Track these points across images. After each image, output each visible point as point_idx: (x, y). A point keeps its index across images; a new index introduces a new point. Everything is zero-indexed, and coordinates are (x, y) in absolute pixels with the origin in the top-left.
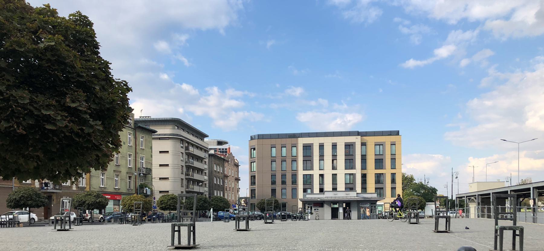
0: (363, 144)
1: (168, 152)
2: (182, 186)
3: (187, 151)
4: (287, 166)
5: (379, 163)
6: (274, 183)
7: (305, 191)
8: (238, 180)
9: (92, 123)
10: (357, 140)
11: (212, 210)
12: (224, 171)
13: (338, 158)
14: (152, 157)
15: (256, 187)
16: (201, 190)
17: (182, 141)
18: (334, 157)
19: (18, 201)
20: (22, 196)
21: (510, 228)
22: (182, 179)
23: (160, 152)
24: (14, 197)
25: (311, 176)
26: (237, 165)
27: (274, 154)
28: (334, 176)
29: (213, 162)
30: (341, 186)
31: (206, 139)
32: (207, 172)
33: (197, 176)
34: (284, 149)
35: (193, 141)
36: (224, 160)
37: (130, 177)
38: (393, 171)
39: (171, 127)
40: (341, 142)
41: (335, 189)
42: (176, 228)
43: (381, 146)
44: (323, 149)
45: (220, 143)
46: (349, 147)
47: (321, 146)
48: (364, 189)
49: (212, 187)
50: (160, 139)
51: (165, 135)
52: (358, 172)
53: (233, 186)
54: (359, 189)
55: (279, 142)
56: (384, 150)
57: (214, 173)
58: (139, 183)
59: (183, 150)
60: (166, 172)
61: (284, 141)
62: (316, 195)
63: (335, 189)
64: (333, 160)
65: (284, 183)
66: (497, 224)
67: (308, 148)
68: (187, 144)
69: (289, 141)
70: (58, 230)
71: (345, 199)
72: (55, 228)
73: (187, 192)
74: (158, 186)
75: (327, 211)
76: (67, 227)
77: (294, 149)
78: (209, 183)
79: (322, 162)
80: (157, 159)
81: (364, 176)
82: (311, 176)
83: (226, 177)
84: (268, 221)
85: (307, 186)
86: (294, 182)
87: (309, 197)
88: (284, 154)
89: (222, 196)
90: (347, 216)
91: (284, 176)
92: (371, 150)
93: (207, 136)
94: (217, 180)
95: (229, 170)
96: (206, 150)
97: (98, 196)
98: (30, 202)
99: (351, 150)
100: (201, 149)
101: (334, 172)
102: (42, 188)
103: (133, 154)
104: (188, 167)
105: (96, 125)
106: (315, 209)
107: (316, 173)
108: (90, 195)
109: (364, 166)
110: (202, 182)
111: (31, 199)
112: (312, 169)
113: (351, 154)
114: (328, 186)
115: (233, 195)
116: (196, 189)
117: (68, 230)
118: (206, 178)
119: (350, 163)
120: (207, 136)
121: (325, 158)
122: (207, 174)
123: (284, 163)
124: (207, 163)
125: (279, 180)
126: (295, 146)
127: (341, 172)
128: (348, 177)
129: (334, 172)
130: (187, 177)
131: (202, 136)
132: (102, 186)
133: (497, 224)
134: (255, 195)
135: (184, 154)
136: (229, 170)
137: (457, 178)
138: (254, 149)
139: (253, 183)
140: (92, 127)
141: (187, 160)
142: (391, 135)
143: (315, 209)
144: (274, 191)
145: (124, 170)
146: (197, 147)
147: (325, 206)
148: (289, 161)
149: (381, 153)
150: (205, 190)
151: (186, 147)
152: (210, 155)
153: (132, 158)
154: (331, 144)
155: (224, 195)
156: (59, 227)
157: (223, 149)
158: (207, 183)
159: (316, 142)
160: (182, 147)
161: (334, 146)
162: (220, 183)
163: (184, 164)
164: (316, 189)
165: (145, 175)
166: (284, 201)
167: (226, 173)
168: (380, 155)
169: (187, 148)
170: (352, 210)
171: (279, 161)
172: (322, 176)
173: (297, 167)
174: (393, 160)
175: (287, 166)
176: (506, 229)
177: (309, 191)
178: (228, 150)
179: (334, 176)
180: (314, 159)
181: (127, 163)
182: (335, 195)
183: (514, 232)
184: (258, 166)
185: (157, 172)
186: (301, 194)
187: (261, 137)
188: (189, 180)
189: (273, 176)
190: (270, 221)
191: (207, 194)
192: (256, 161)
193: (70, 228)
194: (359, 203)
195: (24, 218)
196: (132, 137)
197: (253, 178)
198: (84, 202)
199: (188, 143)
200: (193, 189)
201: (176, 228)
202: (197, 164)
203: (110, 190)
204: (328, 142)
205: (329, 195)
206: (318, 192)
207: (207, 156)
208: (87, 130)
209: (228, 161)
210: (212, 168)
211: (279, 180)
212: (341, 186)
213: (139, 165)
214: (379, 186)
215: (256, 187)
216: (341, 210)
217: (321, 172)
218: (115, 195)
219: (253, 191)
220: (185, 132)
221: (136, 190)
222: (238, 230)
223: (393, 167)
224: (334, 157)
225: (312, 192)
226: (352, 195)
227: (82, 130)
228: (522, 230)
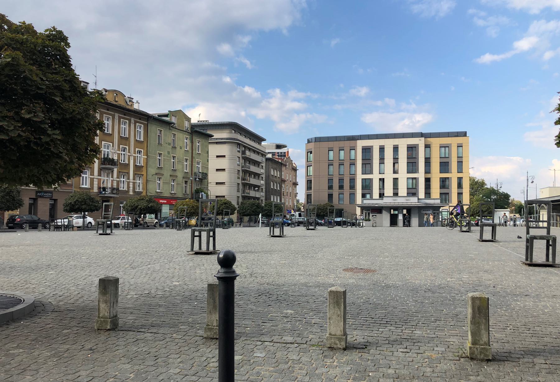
0: (427, 146)
1: (224, 156)
2: (238, 191)
3: (244, 156)
4: (345, 170)
5: (445, 166)
6: (330, 187)
7: (364, 196)
8: (295, 184)
9: (49, 132)
10: (420, 142)
11: (260, 216)
12: (281, 175)
13: (400, 161)
14: (208, 161)
15: (312, 192)
16: (258, 195)
17: (239, 145)
18: (396, 160)
19: (73, 206)
20: (77, 200)
21: (542, 238)
22: (238, 184)
23: (217, 156)
24: (70, 202)
25: (371, 180)
26: (295, 170)
27: (331, 157)
28: (396, 180)
29: (270, 167)
30: (403, 191)
31: (263, 143)
32: (264, 176)
33: (253, 181)
34: (342, 153)
35: (250, 145)
36: (281, 164)
37: (186, 182)
38: (460, 175)
39: (228, 131)
40: (403, 144)
41: (396, 194)
42: (211, 234)
43: (447, 149)
44: (384, 151)
45: (278, 147)
46: (412, 149)
47: (382, 149)
48: (428, 194)
49: (269, 192)
50: (217, 143)
51: (222, 139)
52: (421, 176)
53: (291, 191)
54: (422, 194)
55: (336, 145)
56: (450, 153)
57: (271, 177)
58: (195, 188)
59: (240, 155)
60: (223, 177)
61: (342, 144)
62: (375, 200)
64: (394, 164)
65: (341, 187)
66: (528, 233)
67: (367, 151)
68: (243, 149)
69: (348, 144)
70: (100, 234)
71: (405, 205)
72: (97, 232)
73: (244, 198)
74: (214, 191)
75: (385, 218)
76: (108, 231)
77: (353, 152)
78: (266, 188)
79: (382, 165)
80: (214, 163)
81: (428, 181)
82: (371, 180)
83: (283, 181)
84: (310, 227)
85: (366, 191)
86: (353, 187)
87: (367, 202)
88: (342, 157)
89: (279, 201)
90: (407, 223)
91: (341, 180)
92: (434, 152)
93: (264, 140)
94: (274, 185)
95: (286, 174)
96: (263, 154)
97: (150, 201)
98: (84, 207)
99: (414, 152)
100: (258, 153)
101: (396, 176)
102: (101, 193)
103: (189, 158)
104: (245, 172)
105: (54, 134)
106: (373, 216)
107: (375, 177)
108: (142, 199)
110: (258, 187)
111: (85, 204)
112: (371, 172)
113: (414, 156)
114: (389, 190)
115: (290, 200)
116: (252, 193)
117: (109, 234)
118: (263, 182)
119: (412, 166)
120: (264, 140)
121: (386, 161)
122: (264, 178)
123: (342, 167)
124: (264, 167)
125: (336, 185)
126: (354, 148)
127: (403, 176)
128: (411, 181)
129: (396, 176)
130: (243, 182)
131: (259, 140)
132: (158, 191)
133: (528, 233)
134: (311, 200)
135: (241, 158)
136: (286, 174)
137: (532, 182)
138: (311, 153)
139: (309, 187)
140: (49, 135)
141: (243, 164)
142: (457, 136)
143: (373, 216)
144: (330, 196)
145: (180, 175)
146: (254, 152)
147: (384, 212)
148: (347, 164)
149: (447, 156)
150: (261, 195)
151: (242, 151)
152: (267, 160)
153: (188, 163)
154: (379, 147)
155: (281, 200)
156: (101, 232)
157: (281, 153)
158: (264, 187)
159: (376, 144)
160: (239, 152)
162: (277, 187)
163: (240, 168)
164: (376, 195)
165: (201, 180)
166: (340, 207)
167: (283, 177)
168: (445, 157)
169: (244, 153)
170: (412, 215)
171: (336, 164)
172: (382, 180)
173: (356, 171)
174: (460, 163)
175: (345, 170)
176: (537, 239)
177: (368, 196)
178: (286, 154)
179: (396, 180)
180: (374, 162)
181: (183, 168)
182: (394, 200)
183: (548, 242)
184: (314, 171)
185: (213, 177)
186: (359, 200)
187: (318, 140)
188: (244, 185)
189: (330, 180)
190: (313, 227)
191: (264, 199)
192: (313, 164)
193: (112, 232)
194: (421, 210)
195: (77, 221)
196: (188, 141)
197: (309, 182)
198: (137, 207)
199: (245, 147)
200: (249, 194)
201: (197, 233)
202: (253, 169)
203: (167, 194)
204: (389, 144)
205: (388, 201)
206: (378, 198)
207: (264, 160)
208: (45, 139)
209: (286, 165)
210: (269, 172)
211: (336, 185)
212: (403, 191)
213: (195, 170)
215: (312, 192)
216: (400, 217)
217: (381, 176)
218: (171, 200)
219: (309, 197)
220: (242, 136)
221: (192, 194)
222: (272, 236)
223: (460, 170)
224: (396, 160)
225: (371, 198)
226: (413, 201)
227: (40, 139)
228: (554, 240)
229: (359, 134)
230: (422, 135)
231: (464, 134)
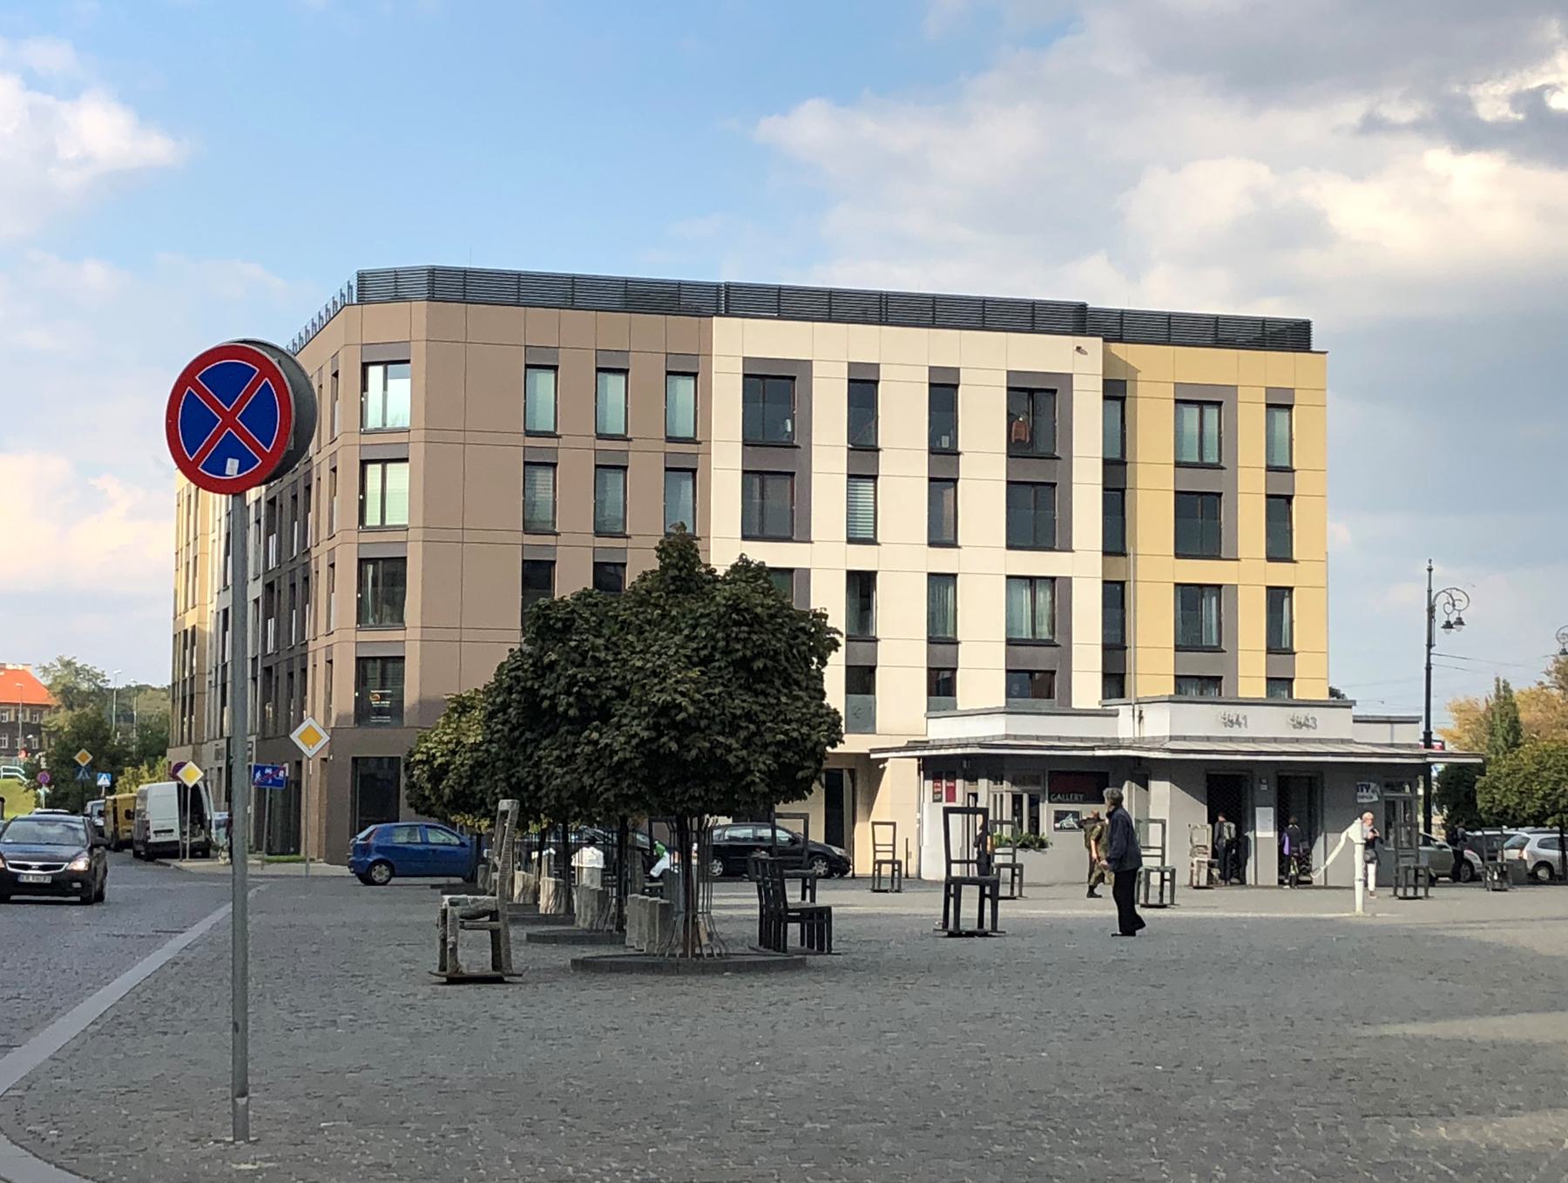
0: (1116, 393)
10: (1079, 362)
38: (1280, 574)
40: (987, 364)
43: (1211, 414)
46: (1034, 407)
47: (863, 389)
52: (1081, 564)
54: (1086, 685)
56: (1227, 439)
61: (617, 330)
63: (1279, 685)
67: (774, 392)
69: (648, 335)
77: (684, 387)
81: (1115, 596)
101: (943, 561)
109: (1116, 543)
127: (985, 559)
129: (943, 561)
149: (1211, 458)
159: (827, 351)
161: (944, 393)
174: (1279, 506)
184: (428, 494)
204: (904, 359)
214: (1200, 664)
217: (862, 559)
223: (1279, 548)
229: (722, 279)
230: (1078, 320)
231: (1294, 337)
